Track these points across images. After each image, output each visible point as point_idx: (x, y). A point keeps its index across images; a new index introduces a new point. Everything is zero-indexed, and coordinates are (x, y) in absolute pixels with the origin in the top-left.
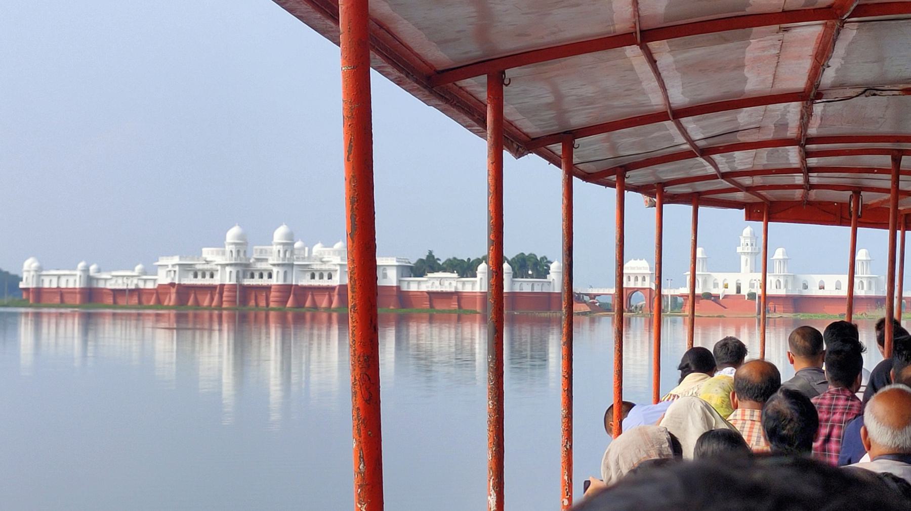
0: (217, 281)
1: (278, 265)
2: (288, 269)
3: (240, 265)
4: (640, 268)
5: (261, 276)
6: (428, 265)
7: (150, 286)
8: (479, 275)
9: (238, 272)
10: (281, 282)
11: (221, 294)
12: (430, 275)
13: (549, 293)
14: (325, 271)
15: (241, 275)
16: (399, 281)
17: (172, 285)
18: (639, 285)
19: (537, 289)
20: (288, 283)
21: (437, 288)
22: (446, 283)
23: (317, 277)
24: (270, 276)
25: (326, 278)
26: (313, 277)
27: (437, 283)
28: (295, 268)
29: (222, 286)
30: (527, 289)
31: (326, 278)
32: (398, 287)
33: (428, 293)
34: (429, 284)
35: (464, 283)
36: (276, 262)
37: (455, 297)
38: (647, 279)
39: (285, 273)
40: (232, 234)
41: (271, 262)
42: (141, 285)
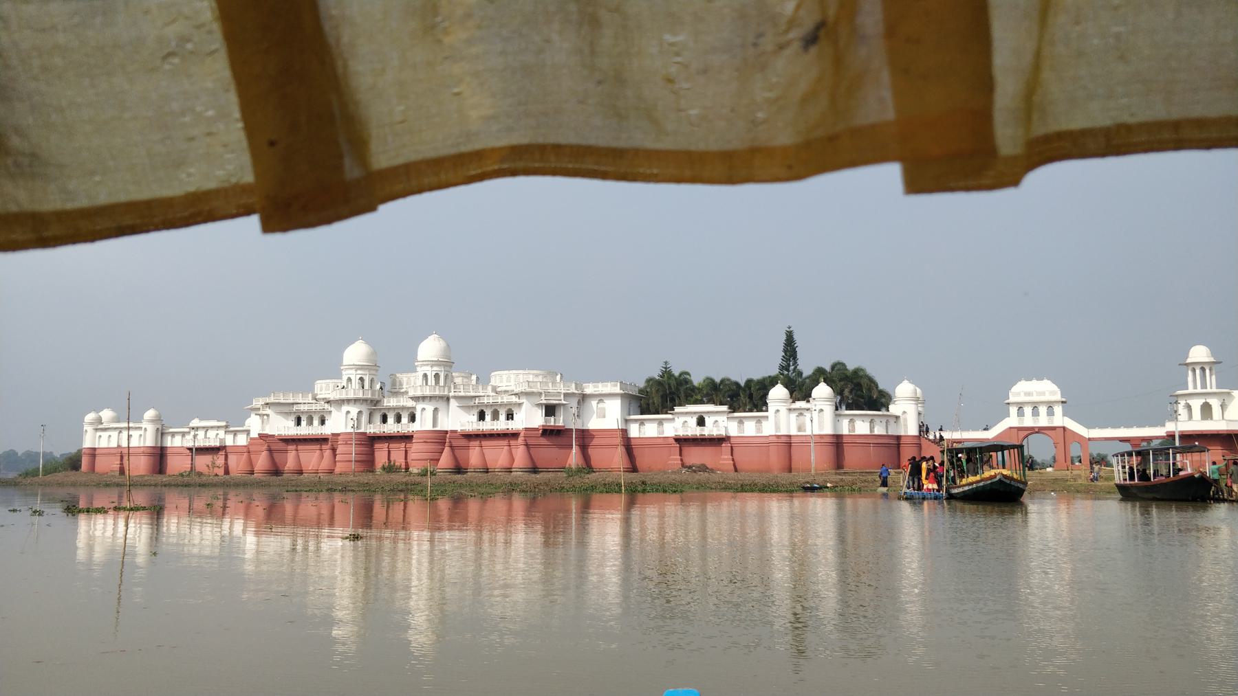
0: (327, 430)
1: (424, 398)
2: (441, 405)
3: (365, 400)
4: (1043, 393)
5: (398, 419)
6: (664, 394)
7: (242, 440)
8: (772, 406)
9: (360, 413)
10: (429, 427)
11: (334, 450)
12: (677, 409)
13: (899, 438)
14: (502, 405)
15: (364, 418)
16: (626, 421)
17: (262, 436)
18: (1043, 421)
19: (879, 430)
20: (438, 428)
21: (692, 430)
22: (709, 421)
23: (488, 417)
24: (413, 418)
25: (503, 417)
26: (482, 416)
27: (693, 421)
28: (452, 401)
29: (335, 435)
30: (862, 428)
31: (503, 417)
32: (624, 432)
33: (678, 440)
34: (679, 421)
35: (741, 421)
36: (419, 393)
37: (725, 447)
38: (1058, 410)
39: (436, 410)
40: (356, 353)
41: (411, 394)
42: (229, 441)
